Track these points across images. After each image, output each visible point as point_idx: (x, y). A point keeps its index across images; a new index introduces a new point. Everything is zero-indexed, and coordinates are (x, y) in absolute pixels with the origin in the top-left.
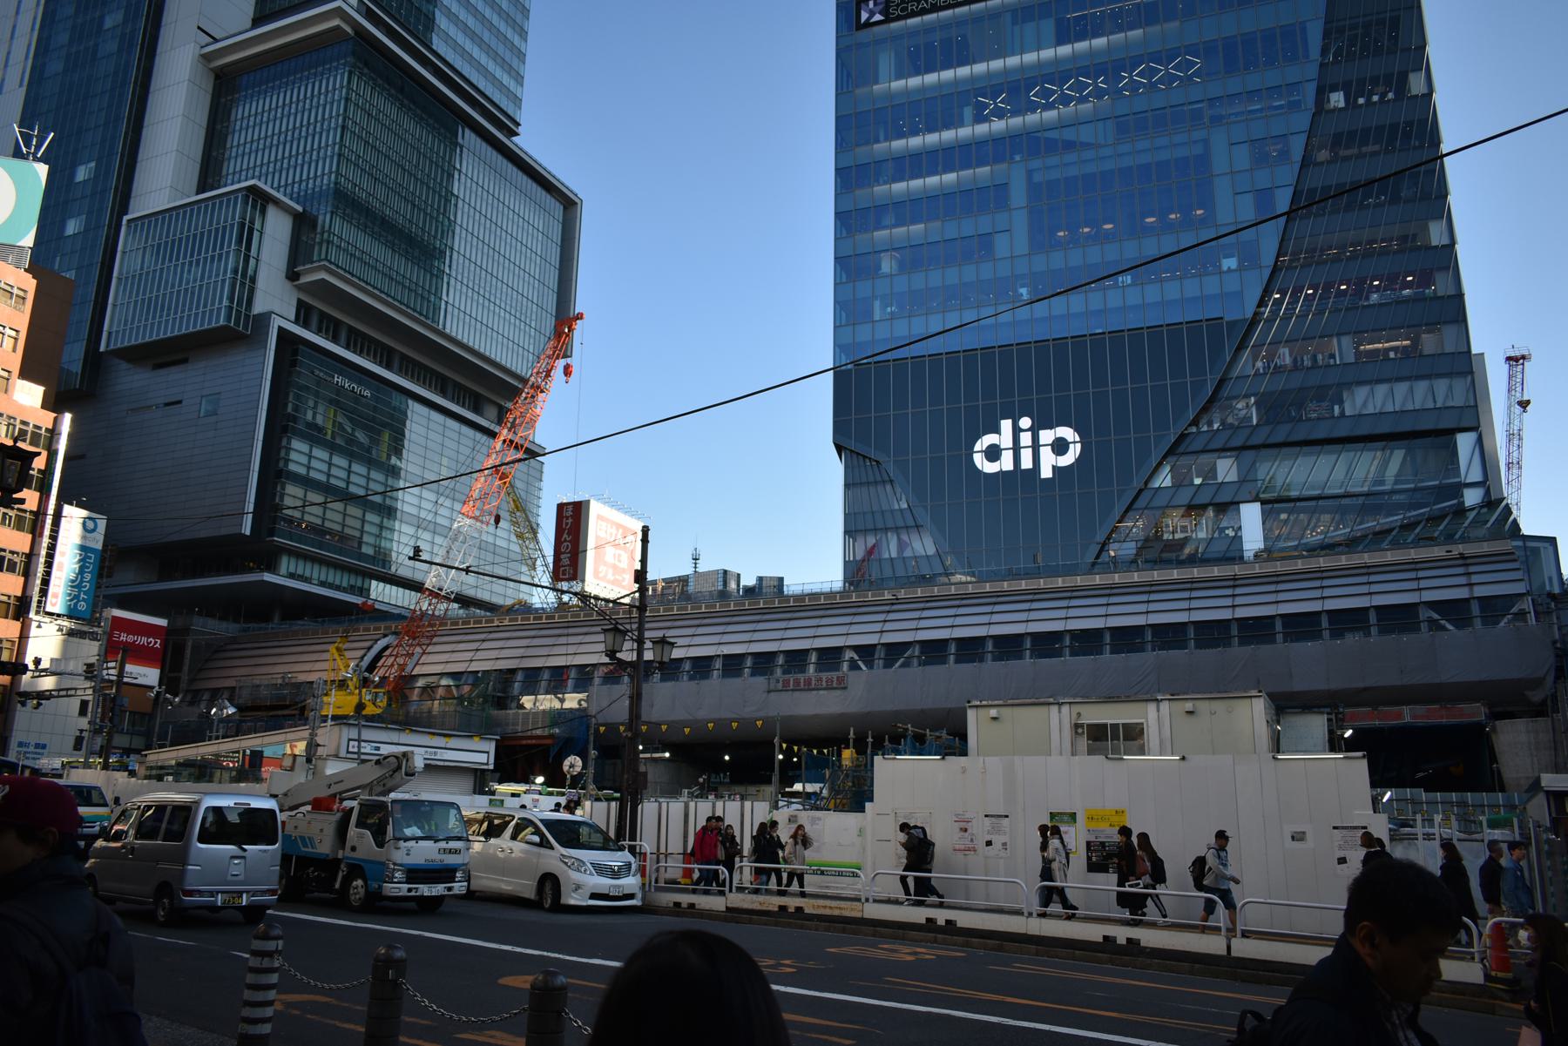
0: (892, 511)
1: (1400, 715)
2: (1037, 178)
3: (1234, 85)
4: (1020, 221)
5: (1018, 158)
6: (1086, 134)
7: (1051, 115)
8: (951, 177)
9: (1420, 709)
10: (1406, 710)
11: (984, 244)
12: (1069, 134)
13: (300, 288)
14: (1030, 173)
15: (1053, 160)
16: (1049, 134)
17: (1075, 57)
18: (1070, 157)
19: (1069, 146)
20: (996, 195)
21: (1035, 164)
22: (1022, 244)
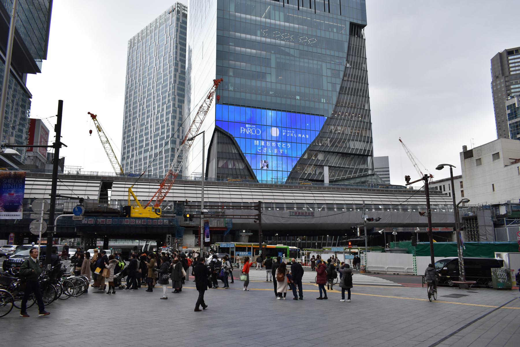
0: (232, 153)
1: (438, 229)
2: (278, 60)
3: (328, 52)
4: (274, 71)
5: (273, 52)
6: (292, 52)
7: (283, 42)
8: (254, 51)
9: (442, 228)
10: (439, 228)
11: (262, 76)
12: (287, 50)
14: (276, 58)
15: (283, 57)
16: (283, 49)
17: (289, 27)
18: (288, 57)
19: (289, 54)
20: (266, 62)
21: (278, 56)
22: (274, 80)
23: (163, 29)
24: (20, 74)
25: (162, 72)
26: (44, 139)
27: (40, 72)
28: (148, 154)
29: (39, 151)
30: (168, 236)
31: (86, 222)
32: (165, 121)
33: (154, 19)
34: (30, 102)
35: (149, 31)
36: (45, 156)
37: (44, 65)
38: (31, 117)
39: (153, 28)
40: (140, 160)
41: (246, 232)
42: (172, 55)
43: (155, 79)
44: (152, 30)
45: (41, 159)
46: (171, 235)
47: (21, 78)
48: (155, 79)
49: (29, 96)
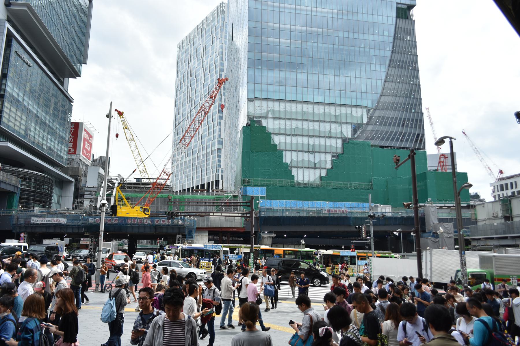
13: (8, 11)
23: (209, 30)
24: (62, 79)
25: (208, 73)
26: (88, 143)
27: (80, 76)
28: (196, 156)
29: (83, 154)
30: (178, 236)
31: (93, 221)
32: (211, 122)
33: (201, 21)
34: (72, 106)
35: (196, 34)
36: (89, 159)
37: (85, 70)
38: (72, 121)
39: (200, 30)
40: (189, 161)
41: (268, 233)
42: (218, 55)
43: (202, 81)
44: (199, 32)
45: (85, 162)
46: (181, 236)
47: (62, 83)
48: (202, 81)
49: (70, 100)
